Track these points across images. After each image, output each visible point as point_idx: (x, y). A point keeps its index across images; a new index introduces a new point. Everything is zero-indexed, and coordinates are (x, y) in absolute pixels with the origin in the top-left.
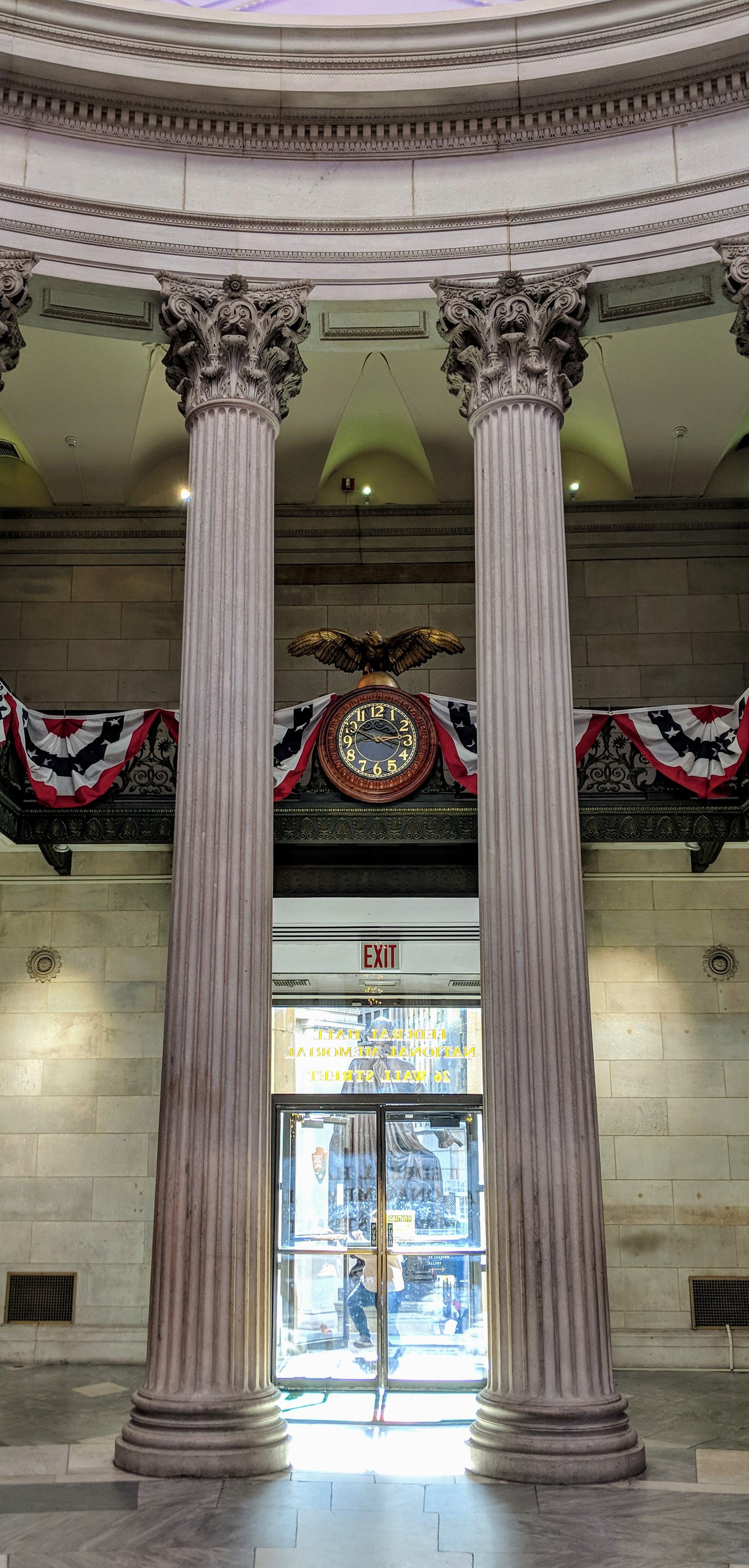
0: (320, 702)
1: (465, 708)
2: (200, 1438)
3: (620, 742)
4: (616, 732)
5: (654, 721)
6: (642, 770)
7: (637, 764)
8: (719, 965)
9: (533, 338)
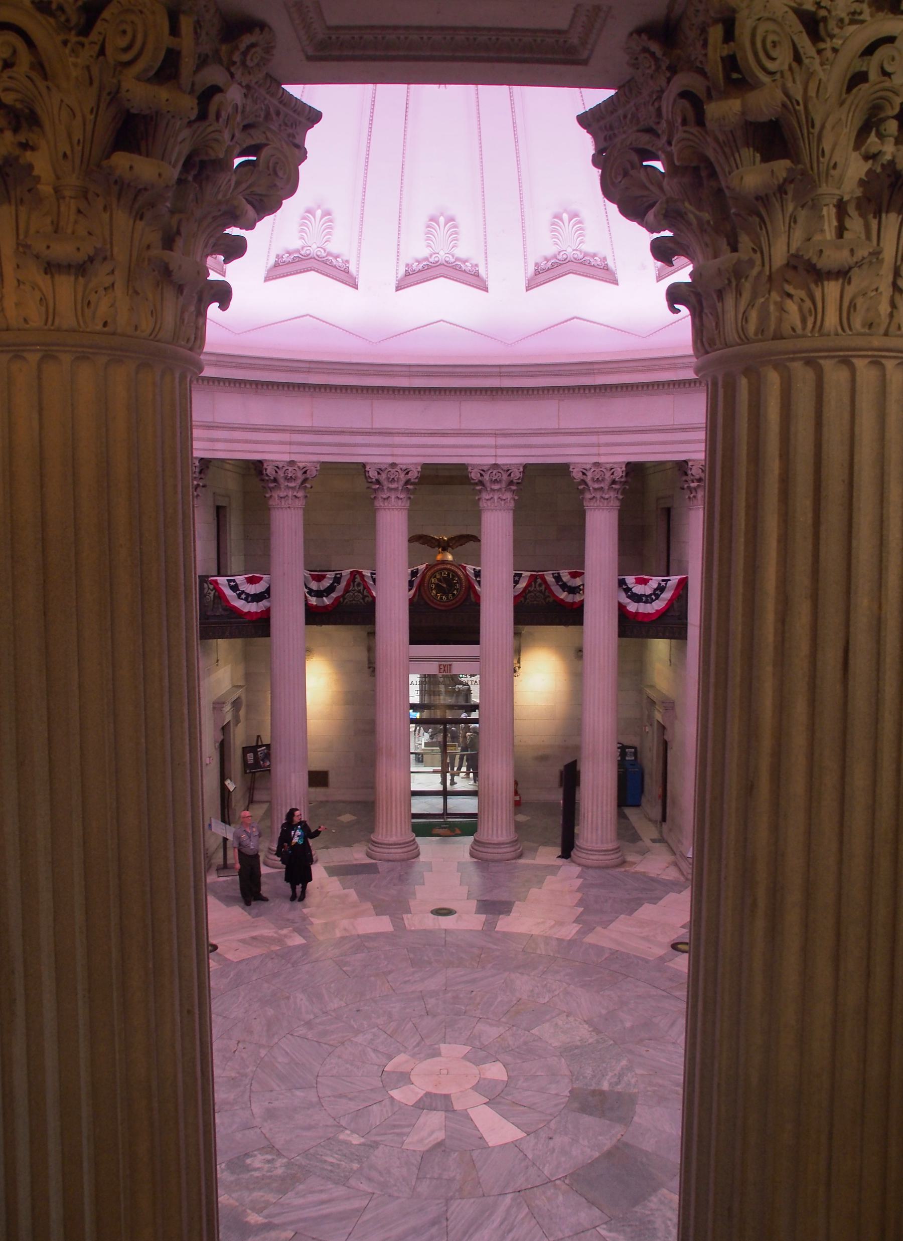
0: (422, 567)
1: (480, 571)
2: (393, 851)
3: (540, 585)
4: (539, 581)
5: (554, 577)
6: (549, 597)
7: (547, 593)
8: (580, 653)
9: (504, 485)
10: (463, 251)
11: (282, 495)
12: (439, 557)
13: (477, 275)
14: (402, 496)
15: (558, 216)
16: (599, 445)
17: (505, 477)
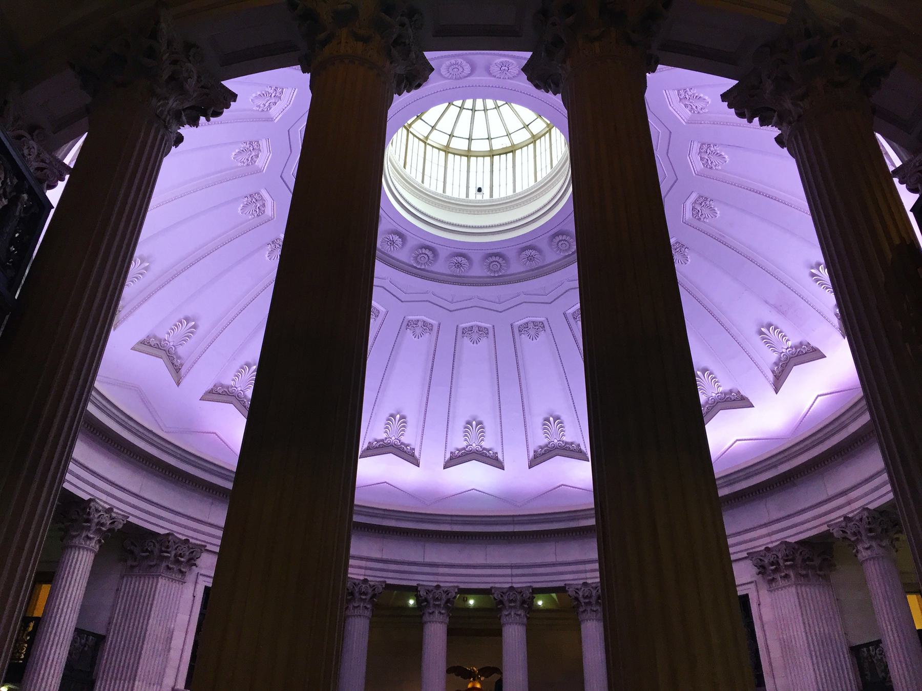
9: (518, 603)
10: (487, 443)
11: (356, 605)
12: (470, 686)
13: (497, 459)
14: (443, 612)
15: (547, 420)
16: (586, 572)
17: (519, 597)
